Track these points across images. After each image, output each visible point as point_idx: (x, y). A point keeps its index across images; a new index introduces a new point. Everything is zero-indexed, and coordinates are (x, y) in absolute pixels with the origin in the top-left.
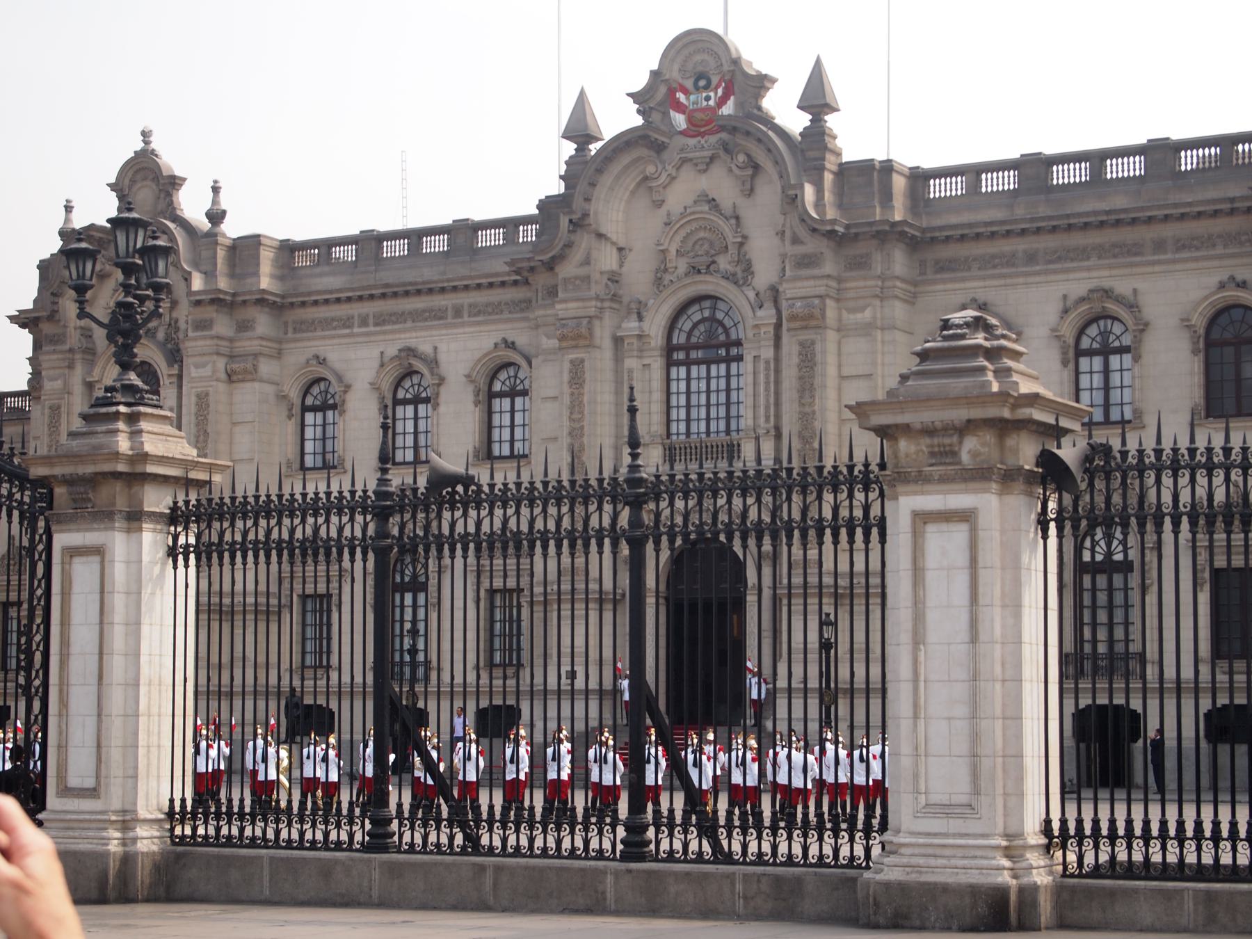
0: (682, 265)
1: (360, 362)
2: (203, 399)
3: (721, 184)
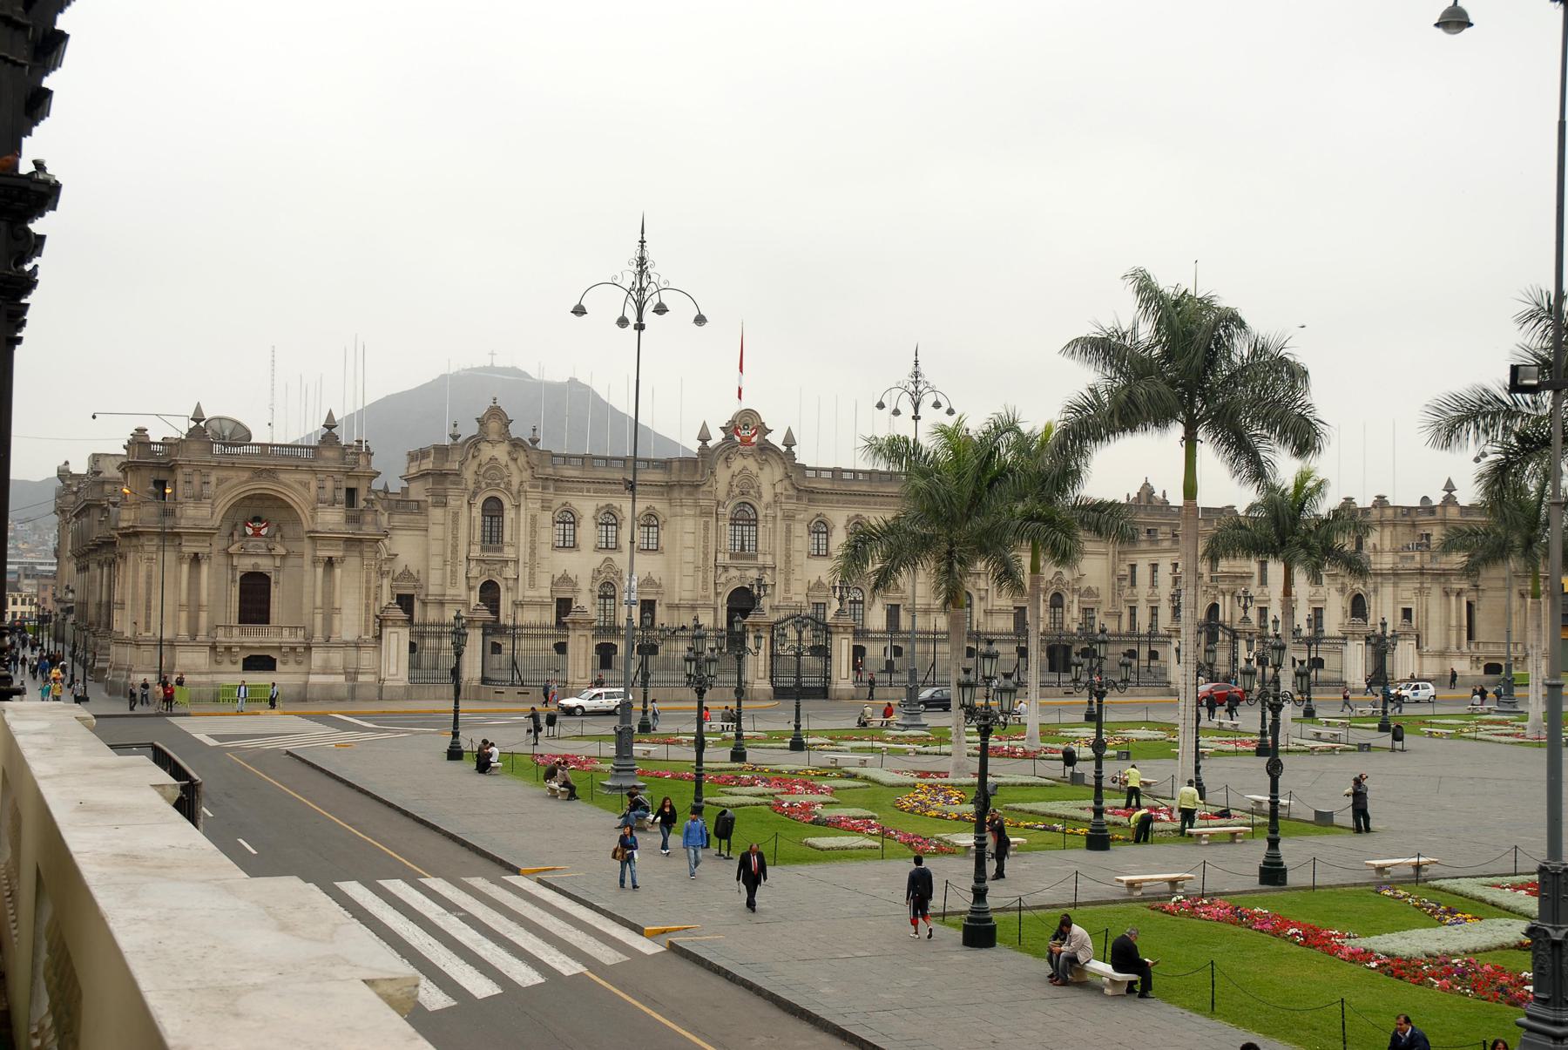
0: (737, 491)
1: (587, 507)
2: (534, 518)
3: (751, 465)
